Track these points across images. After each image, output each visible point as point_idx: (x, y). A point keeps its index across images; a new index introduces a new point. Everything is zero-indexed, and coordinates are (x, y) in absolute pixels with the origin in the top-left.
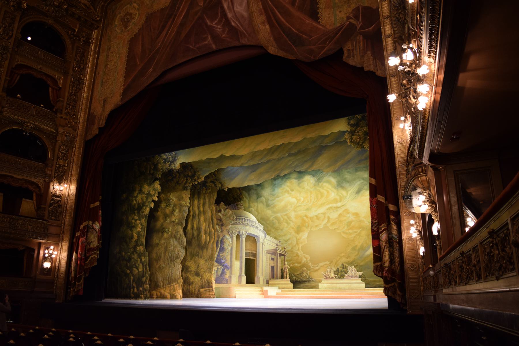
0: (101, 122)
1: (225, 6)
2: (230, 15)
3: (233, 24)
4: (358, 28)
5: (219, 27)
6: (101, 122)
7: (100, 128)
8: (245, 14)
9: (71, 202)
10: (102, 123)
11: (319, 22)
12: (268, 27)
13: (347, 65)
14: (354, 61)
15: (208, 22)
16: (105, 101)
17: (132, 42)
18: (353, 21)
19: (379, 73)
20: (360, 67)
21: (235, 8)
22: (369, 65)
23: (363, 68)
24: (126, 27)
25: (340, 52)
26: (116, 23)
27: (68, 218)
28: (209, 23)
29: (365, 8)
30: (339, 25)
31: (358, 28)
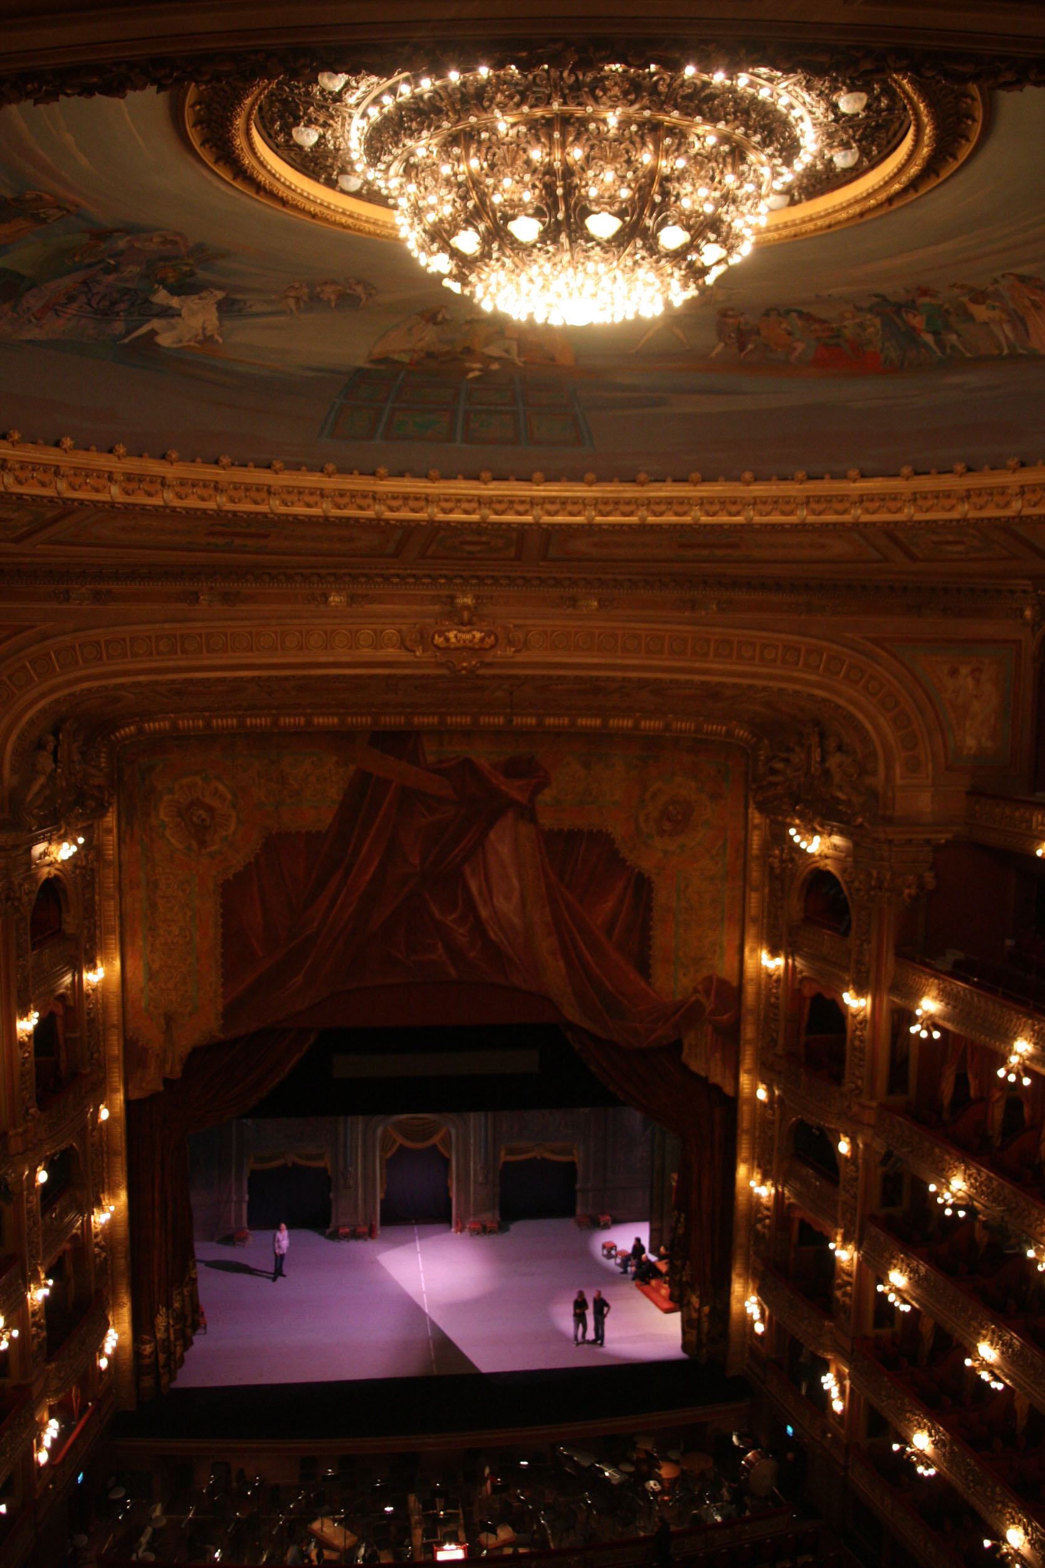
0: (168, 1067)
1: (474, 888)
2: (484, 913)
3: (492, 935)
4: (708, 1011)
5: (461, 931)
6: (168, 1067)
7: (167, 1082)
8: (516, 921)
9: (122, 1231)
10: (175, 1071)
11: (649, 984)
12: (562, 964)
13: (685, 1068)
14: (697, 1066)
15: (434, 909)
16: (169, 1019)
17: (232, 893)
18: (704, 1001)
19: (728, 1090)
20: (703, 1074)
21: (495, 901)
22: (717, 1075)
23: (706, 1079)
24: (202, 843)
25: (678, 1045)
26: (162, 816)
27: (122, 1263)
28: (438, 915)
29: (723, 983)
30: (679, 997)
31: (708, 1011)
